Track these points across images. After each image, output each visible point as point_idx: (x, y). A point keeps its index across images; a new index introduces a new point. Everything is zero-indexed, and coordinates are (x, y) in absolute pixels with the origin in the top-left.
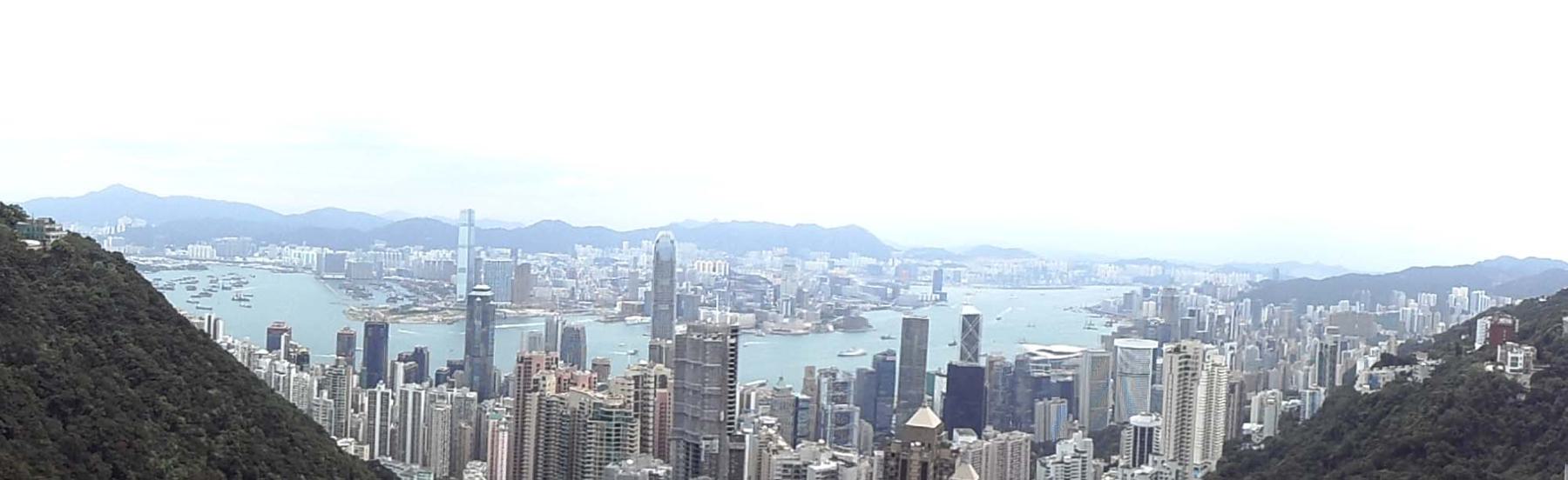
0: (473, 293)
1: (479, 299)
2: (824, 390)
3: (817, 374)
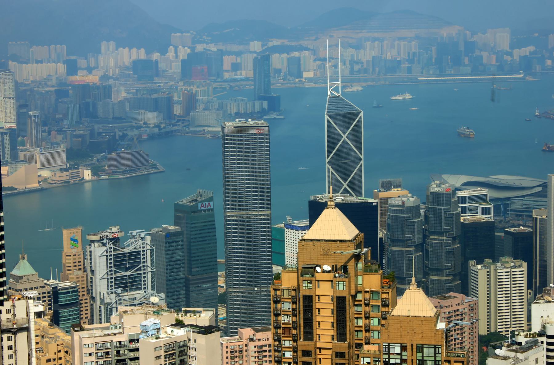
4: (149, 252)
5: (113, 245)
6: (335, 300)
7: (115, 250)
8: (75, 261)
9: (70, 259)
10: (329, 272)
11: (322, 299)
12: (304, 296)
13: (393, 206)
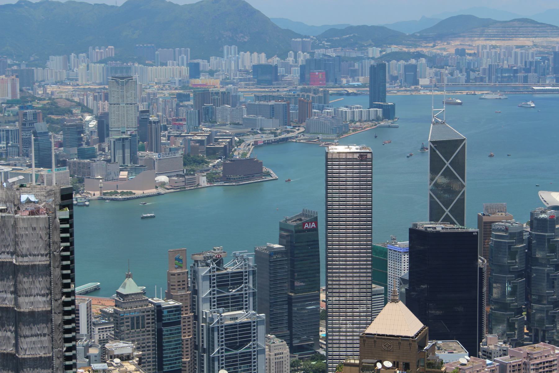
5: (217, 265)
7: (218, 270)
8: (179, 280)
9: (175, 278)
10: (389, 368)
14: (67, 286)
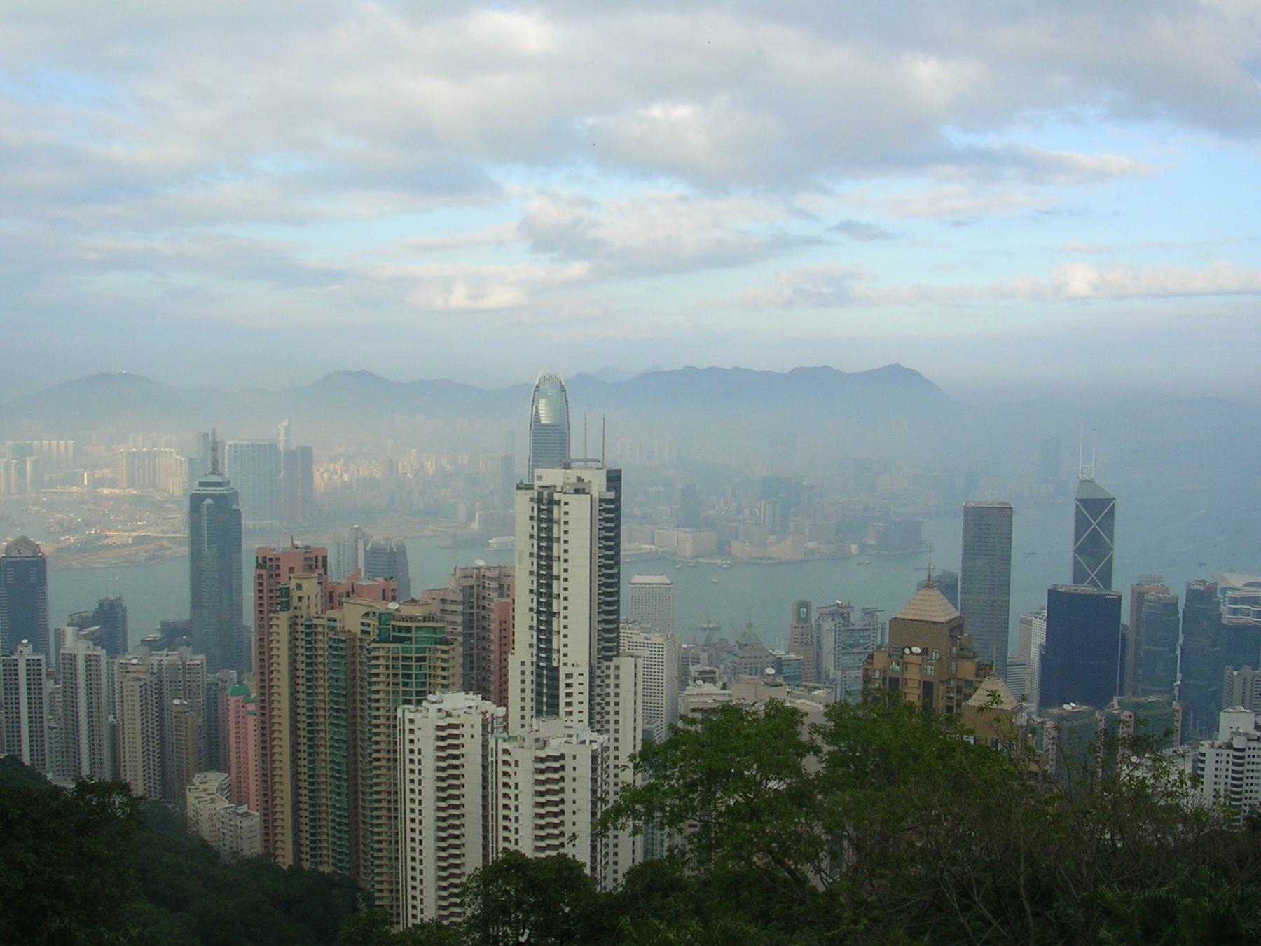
0: (203, 490)
1: (209, 501)
2: (829, 643)
3: (814, 615)
4: (879, 630)
6: (922, 684)
7: (844, 625)
10: (918, 654)
11: (910, 684)
12: (891, 679)
13: (1147, 601)
14: (610, 567)
